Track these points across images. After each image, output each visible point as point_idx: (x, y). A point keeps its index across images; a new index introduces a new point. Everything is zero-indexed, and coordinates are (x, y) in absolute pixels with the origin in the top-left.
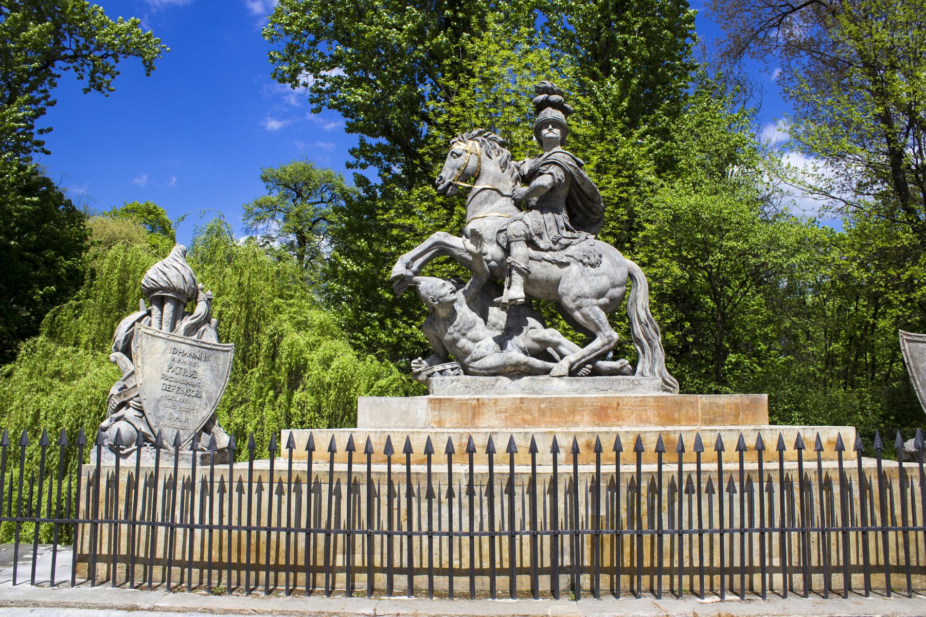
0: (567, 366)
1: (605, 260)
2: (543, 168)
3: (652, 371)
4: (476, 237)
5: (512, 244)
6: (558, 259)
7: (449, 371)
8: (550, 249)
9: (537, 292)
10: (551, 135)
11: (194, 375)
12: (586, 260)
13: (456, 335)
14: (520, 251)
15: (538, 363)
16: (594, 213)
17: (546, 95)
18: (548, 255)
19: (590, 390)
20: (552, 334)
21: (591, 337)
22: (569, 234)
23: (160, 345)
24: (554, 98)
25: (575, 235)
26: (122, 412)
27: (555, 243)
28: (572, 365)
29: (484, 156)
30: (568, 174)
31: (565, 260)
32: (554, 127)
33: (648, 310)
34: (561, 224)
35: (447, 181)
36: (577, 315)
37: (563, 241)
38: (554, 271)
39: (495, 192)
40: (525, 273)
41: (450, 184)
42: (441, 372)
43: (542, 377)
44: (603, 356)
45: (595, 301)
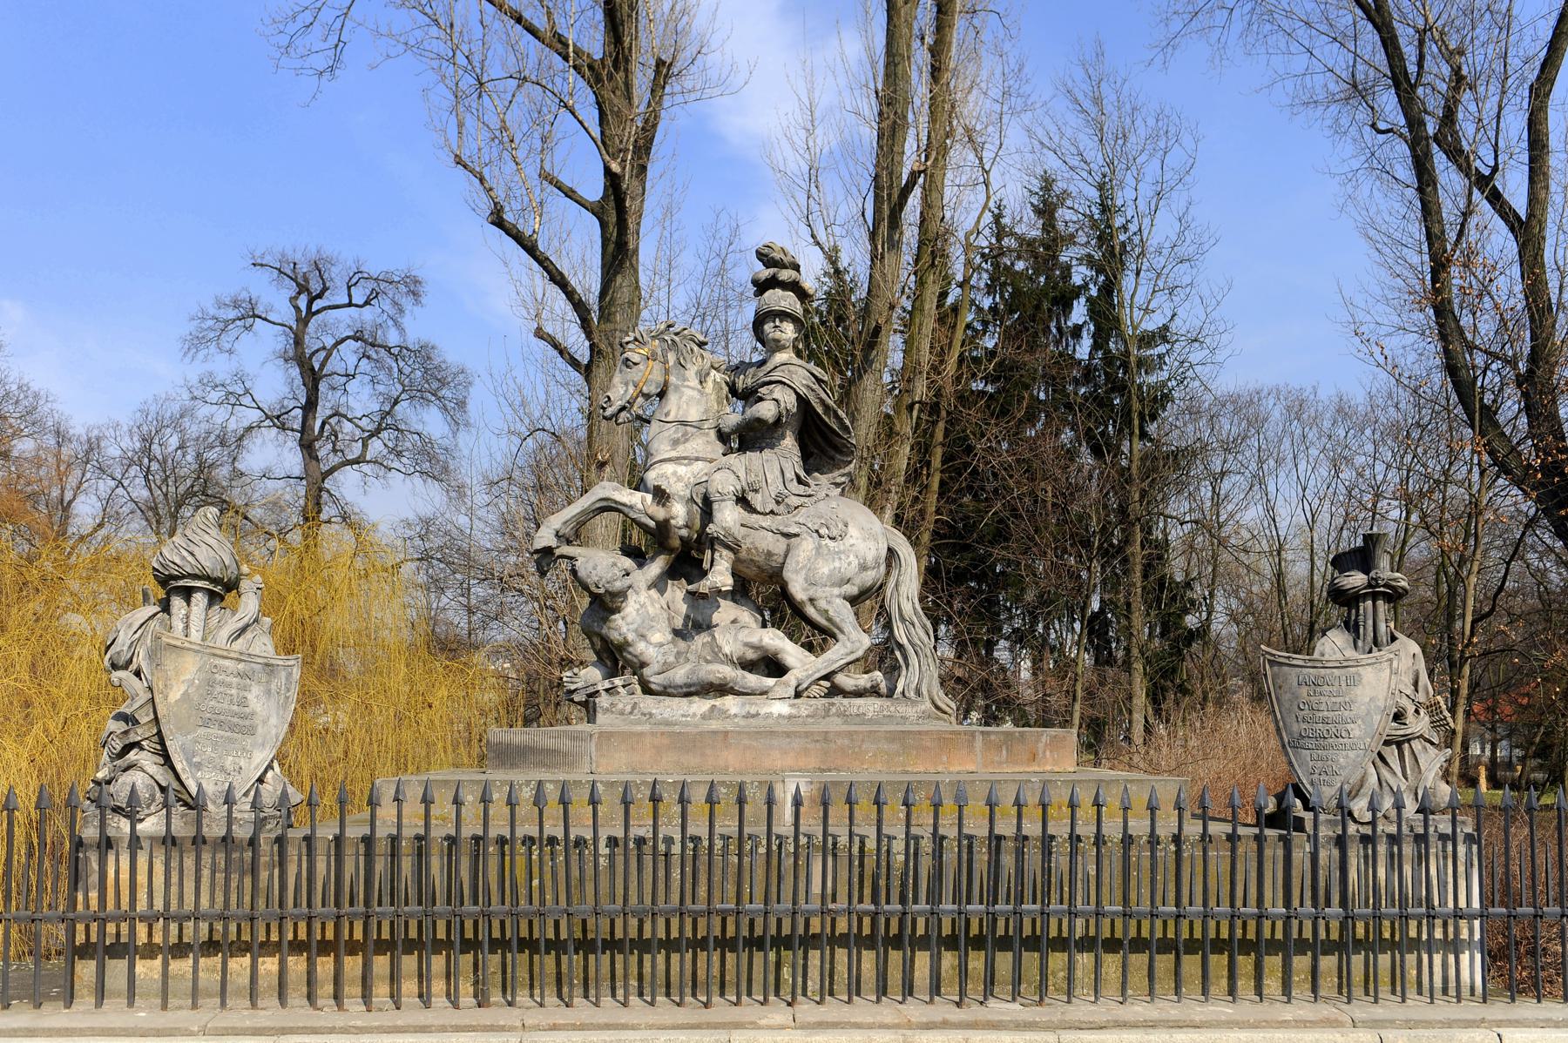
0: (794, 683)
1: (852, 530)
2: (763, 390)
3: (918, 692)
4: (661, 495)
5: (715, 506)
7: (621, 690)
8: (772, 512)
9: (750, 572)
10: (778, 335)
11: (243, 702)
12: (823, 531)
13: (630, 637)
14: (728, 516)
15: (753, 680)
16: (841, 452)
17: (772, 271)
18: (767, 522)
20: (774, 639)
22: (801, 489)
24: (785, 275)
25: (810, 491)
26: (132, 755)
27: (778, 503)
30: (802, 401)
31: (793, 530)
33: (916, 601)
34: (790, 475)
36: (811, 611)
37: (794, 501)
38: (778, 546)
40: (734, 548)
42: (607, 690)
45: (836, 591)
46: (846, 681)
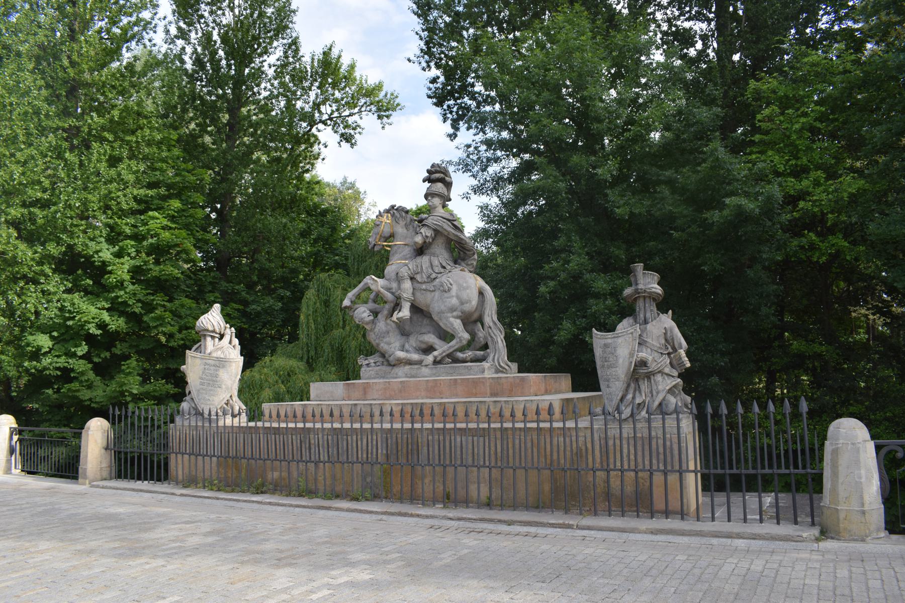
6: (428, 288)
8: (425, 282)
18: (424, 287)
19: (445, 375)
21: (452, 337)
23: (198, 361)
28: (435, 357)
32: (433, 197)
37: (434, 276)
43: (416, 367)
44: (462, 349)
45: (449, 315)
46: (460, 355)
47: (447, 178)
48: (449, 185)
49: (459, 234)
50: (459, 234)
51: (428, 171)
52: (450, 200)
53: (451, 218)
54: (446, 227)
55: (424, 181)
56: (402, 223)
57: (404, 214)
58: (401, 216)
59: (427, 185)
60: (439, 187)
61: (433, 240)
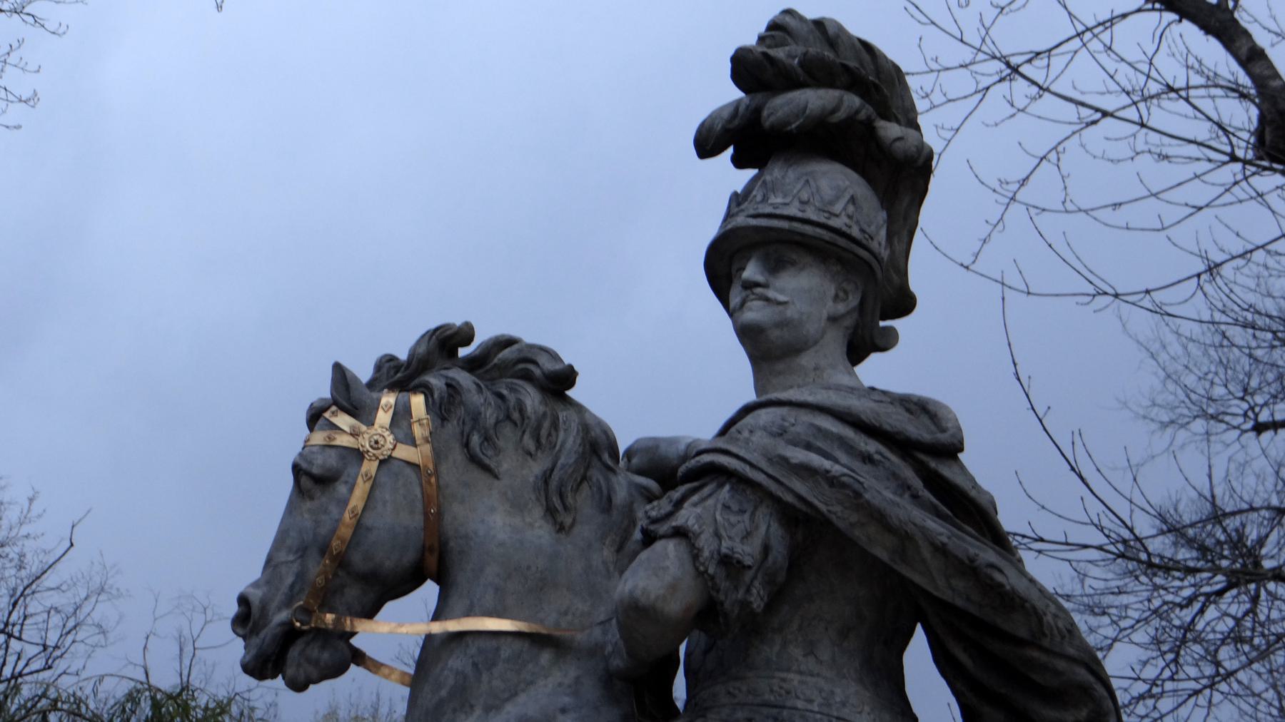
29: (455, 469)
32: (775, 266)
35: (283, 615)
39: (507, 649)
41: (290, 635)
47: (890, 130)
48: (903, 178)
49: (987, 555)
50: (987, 555)
51: (745, 68)
52: (904, 303)
53: (915, 429)
54: (880, 492)
55: (707, 145)
56: (518, 468)
57: (532, 399)
58: (513, 416)
59: (725, 176)
60: (827, 192)
61: (776, 597)
